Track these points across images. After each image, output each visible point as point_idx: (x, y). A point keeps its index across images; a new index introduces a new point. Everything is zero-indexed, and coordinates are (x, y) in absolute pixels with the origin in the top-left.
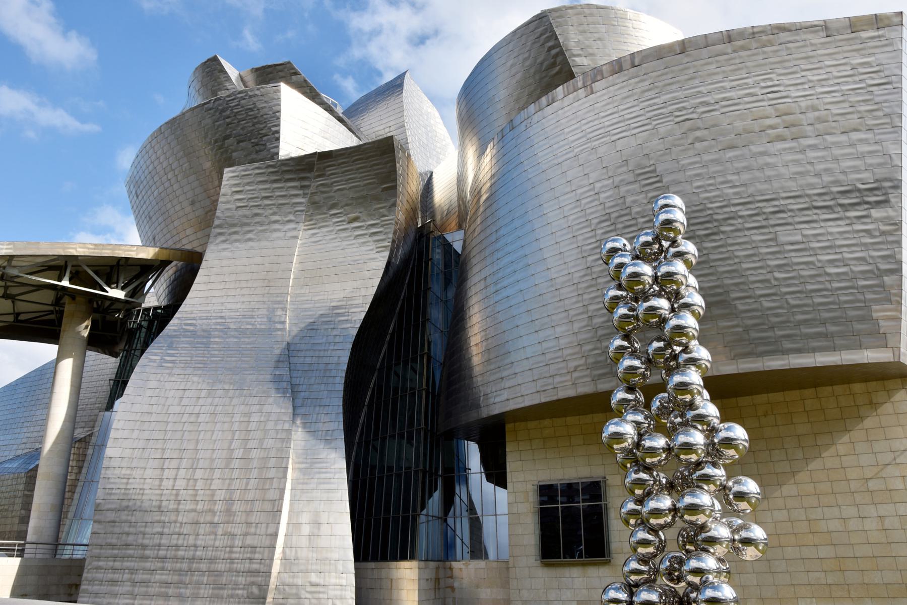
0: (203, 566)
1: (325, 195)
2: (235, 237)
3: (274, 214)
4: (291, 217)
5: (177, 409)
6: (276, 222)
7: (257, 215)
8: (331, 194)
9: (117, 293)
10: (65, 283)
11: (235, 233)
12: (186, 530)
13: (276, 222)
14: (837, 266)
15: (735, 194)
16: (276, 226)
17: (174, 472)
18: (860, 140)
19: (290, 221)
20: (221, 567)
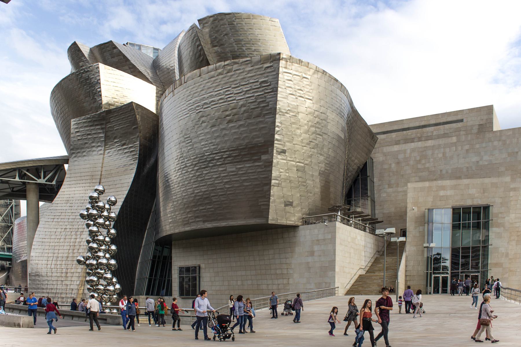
0: (59, 296)
1: (112, 132)
2: (79, 154)
3: (93, 142)
4: (99, 144)
5: (53, 237)
6: (94, 146)
7: (86, 143)
8: (114, 132)
11: (79, 152)
12: (54, 283)
13: (94, 146)
14: (247, 182)
15: (214, 148)
16: (94, 149)
17: (51, 262)
18: (260, 122)
19: (99, 146)
20: (63, 296)
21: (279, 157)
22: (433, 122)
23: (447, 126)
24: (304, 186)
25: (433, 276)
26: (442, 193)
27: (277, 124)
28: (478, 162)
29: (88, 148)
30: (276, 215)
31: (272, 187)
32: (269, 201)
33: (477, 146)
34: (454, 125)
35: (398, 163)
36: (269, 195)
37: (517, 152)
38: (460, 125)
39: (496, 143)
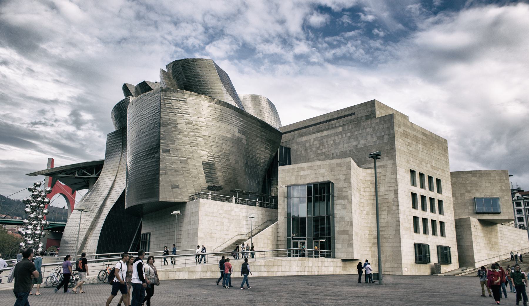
9: (94, 176)
10: (77, 175)
21: (165, 154)
22: (335, 116)
23: (345, 119)
24: (188, 173)
25: (292, 241)
26: (301, 173)
27: (162, 133)
28: (357, 145)
29: (114, 152)
30: (165, 195)
31: (160, 176)
32: (159, 185)
33: (356, 133)
34: (349, 118)
35: (306, 150)
36: (159, 181)
37: (383, 136)
38: (353, 117)
39: (368, 130)
